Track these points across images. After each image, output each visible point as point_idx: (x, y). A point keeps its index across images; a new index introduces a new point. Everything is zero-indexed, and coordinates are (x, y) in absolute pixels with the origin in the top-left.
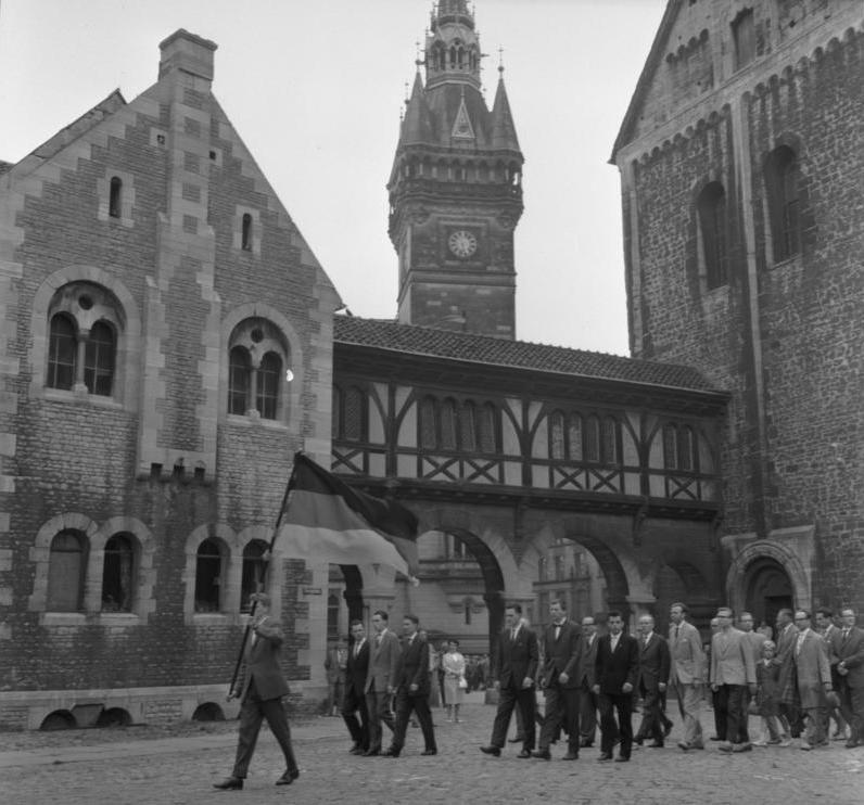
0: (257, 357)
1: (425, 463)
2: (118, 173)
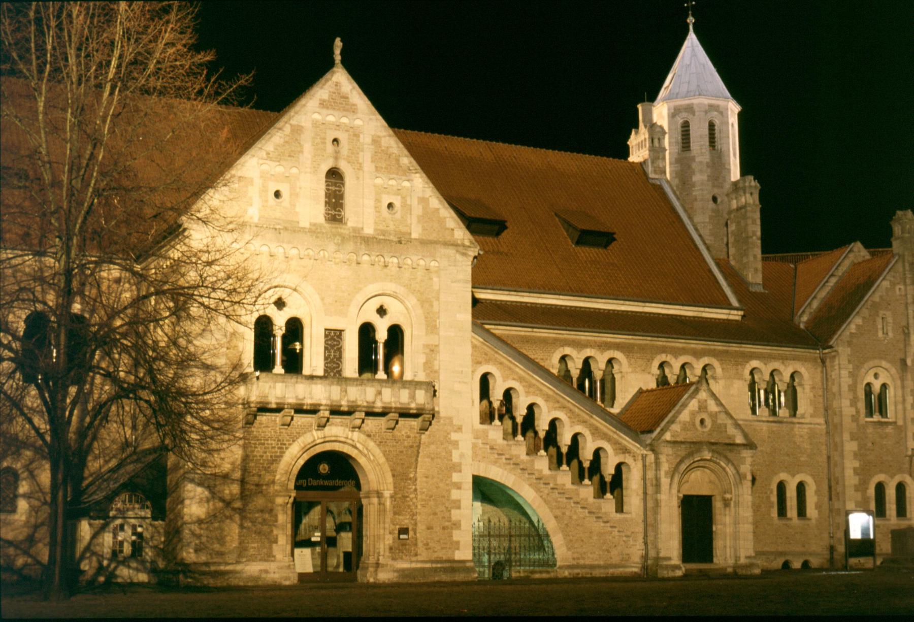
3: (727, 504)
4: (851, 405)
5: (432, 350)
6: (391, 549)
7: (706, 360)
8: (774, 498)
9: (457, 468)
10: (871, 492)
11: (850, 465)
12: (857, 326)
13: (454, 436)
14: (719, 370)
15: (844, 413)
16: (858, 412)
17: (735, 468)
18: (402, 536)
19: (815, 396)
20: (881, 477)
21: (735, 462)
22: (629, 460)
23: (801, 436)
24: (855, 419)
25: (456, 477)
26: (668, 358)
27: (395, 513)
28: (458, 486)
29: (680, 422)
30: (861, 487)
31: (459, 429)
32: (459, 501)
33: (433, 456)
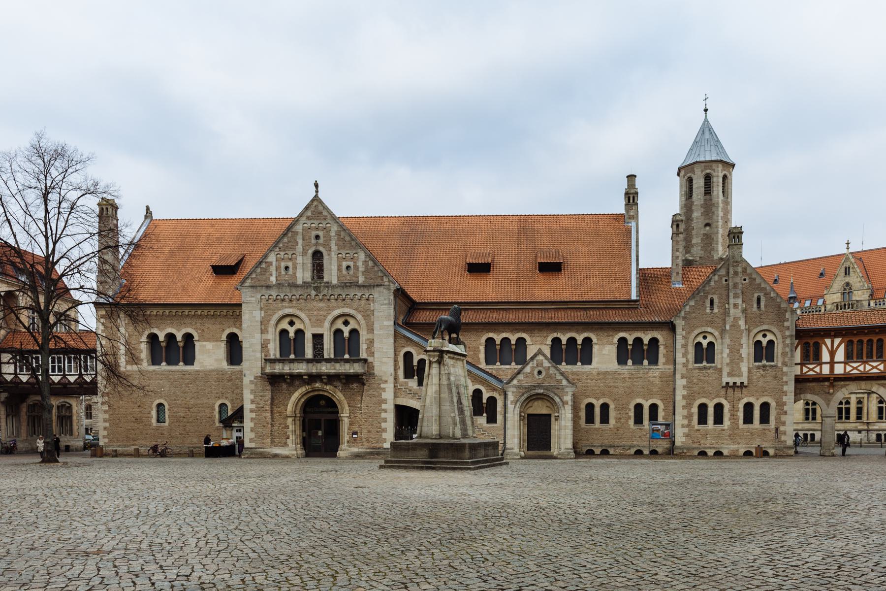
0: (764, 343)
1: (818, 371)
2: (712, 296)
3: (557, 418)
4: (683, 357)
5: (371, 342)
6: (348, 442)
7: (585, 335)
8: (632, 414)
9: (385, 401)
10: (695, 410)
11: (680, 393)
12: (691, 307)
13: (383, 386)
14: (595, 340)
15: (677, 362)
16: (688, 361)
17: (560, 398)
18: (354, 436)
19: (667, 352)
20: (703, 400)
21: (560, 395)
22: (495, 395)
23: (654, 377)
24: (685, 365)
25: (384, 406)
26: (559, 335)
27: (350, 424)
28: (385, 411)
29: (524, 373)
30: (688, 406)
31: (386, 382)
32: (386, 418)
33: (371, 396)
